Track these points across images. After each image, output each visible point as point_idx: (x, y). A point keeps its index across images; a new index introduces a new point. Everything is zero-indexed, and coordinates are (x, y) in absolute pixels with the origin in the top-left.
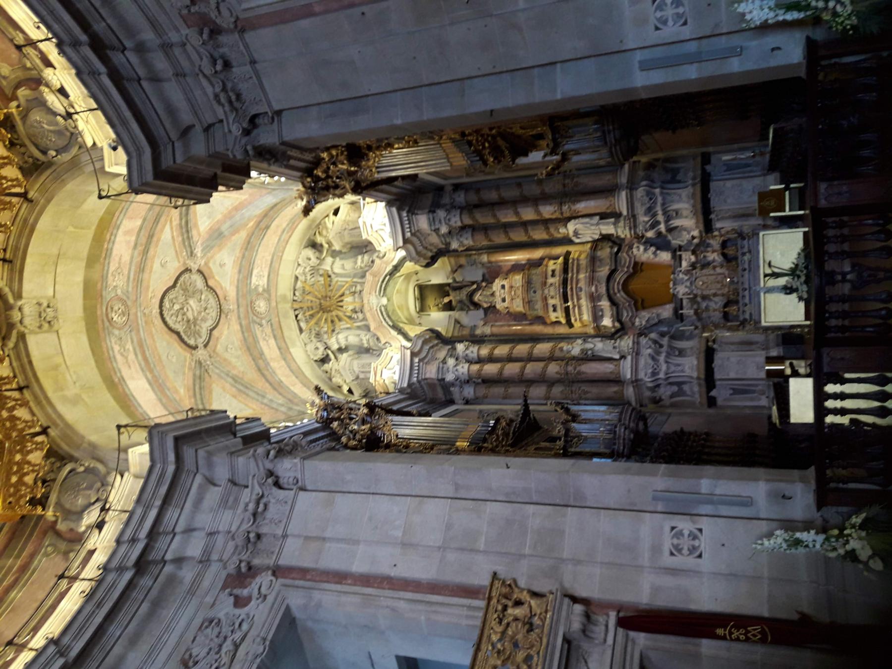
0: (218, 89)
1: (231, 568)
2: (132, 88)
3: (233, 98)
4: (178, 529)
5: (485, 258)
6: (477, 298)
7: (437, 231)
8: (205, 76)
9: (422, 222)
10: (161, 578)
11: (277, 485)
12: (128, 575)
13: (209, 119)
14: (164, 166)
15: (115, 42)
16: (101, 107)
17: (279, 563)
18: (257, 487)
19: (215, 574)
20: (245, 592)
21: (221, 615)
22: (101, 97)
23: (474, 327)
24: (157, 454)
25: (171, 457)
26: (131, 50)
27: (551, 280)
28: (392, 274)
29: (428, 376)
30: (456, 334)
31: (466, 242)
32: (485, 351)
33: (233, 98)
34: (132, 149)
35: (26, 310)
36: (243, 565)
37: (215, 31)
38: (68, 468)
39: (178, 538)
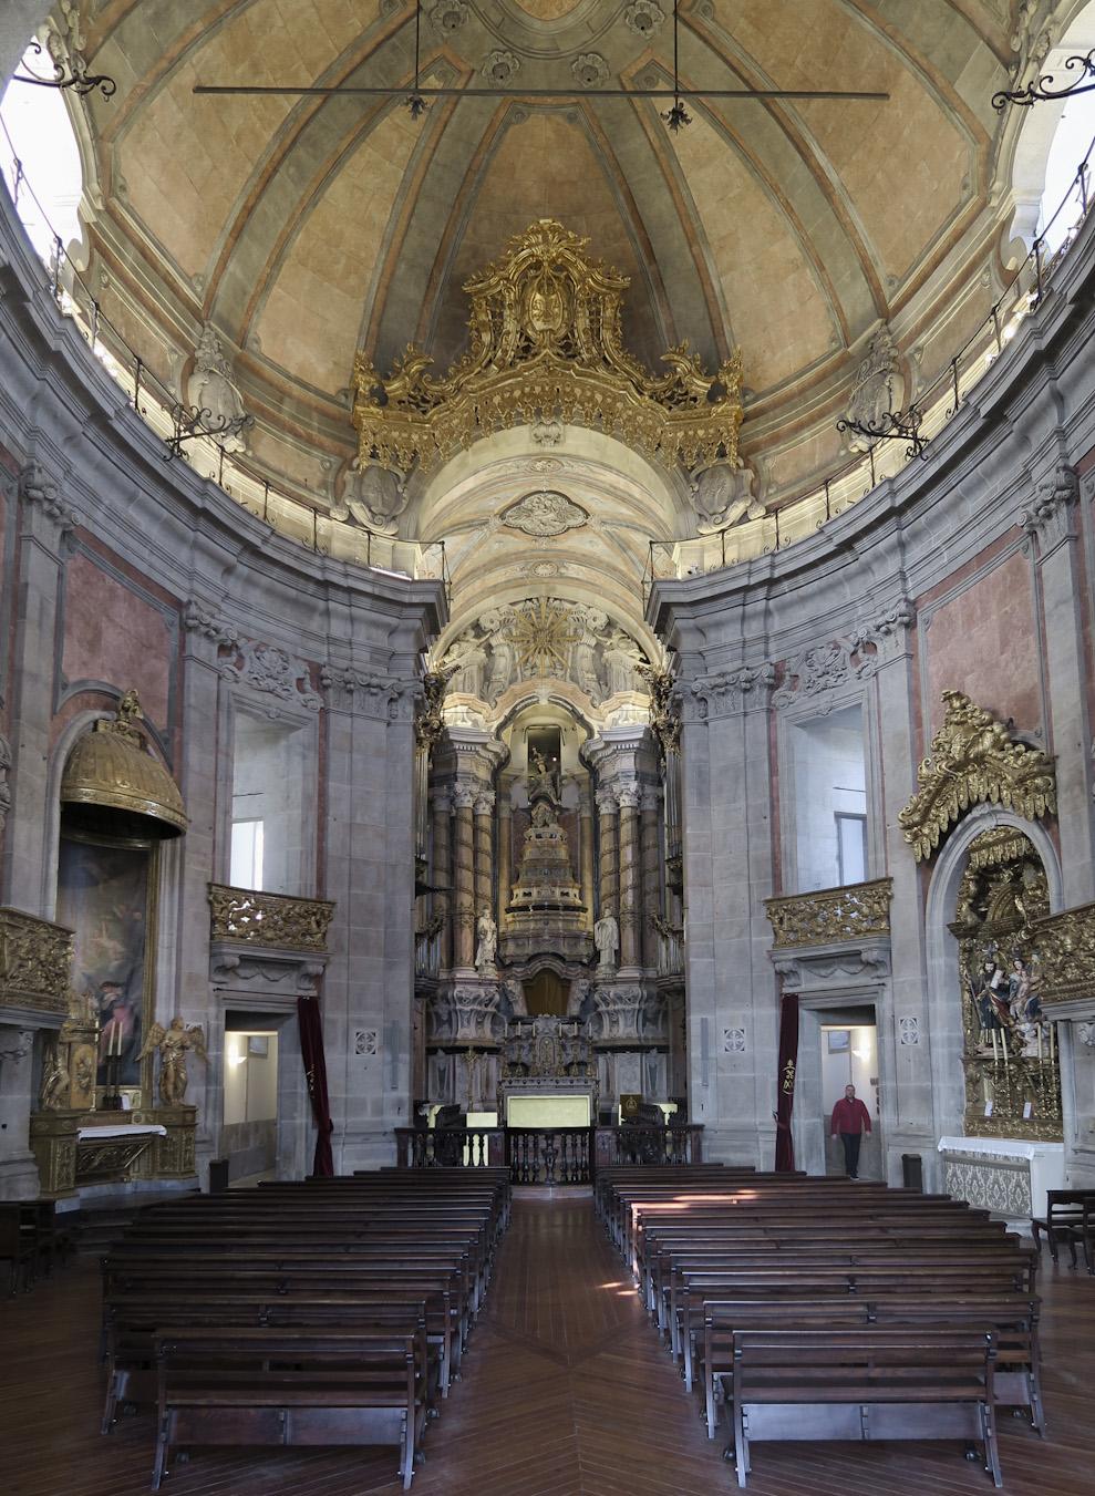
0: (728, 678)
1: (325, 671)
2: (738, 598)
3: (722, 690)
4: (354, 610)
5: (586, 814)
6: (542, 805)
7: (616, 778)
8: (740, 669)
9: (627, 763)
10: (314, 601)
11: (391, 700)
12: (318, 575)
13: (710, 658)
14: (673, 609)
15: (773, 594)
16: (725, 568)
17: (332, 715)
18: (390, 683)
19: (321, 652)
20: (308, 687)
21: (291, 669)
22: (730, 574)
23: (509, 798)
24: (418, 587)
25: (416, 599)
26: (767, 605)
27: (558, 891)
28: (574, 711)
29: (460, 760)
30: (502, 777)
31: (603, 806)
32: (485, 822)
33: (722, 690)
34: (690, 585)
36: (329, 682)
37: (772, 688)
38: (402, 475)
39: (346, 610)
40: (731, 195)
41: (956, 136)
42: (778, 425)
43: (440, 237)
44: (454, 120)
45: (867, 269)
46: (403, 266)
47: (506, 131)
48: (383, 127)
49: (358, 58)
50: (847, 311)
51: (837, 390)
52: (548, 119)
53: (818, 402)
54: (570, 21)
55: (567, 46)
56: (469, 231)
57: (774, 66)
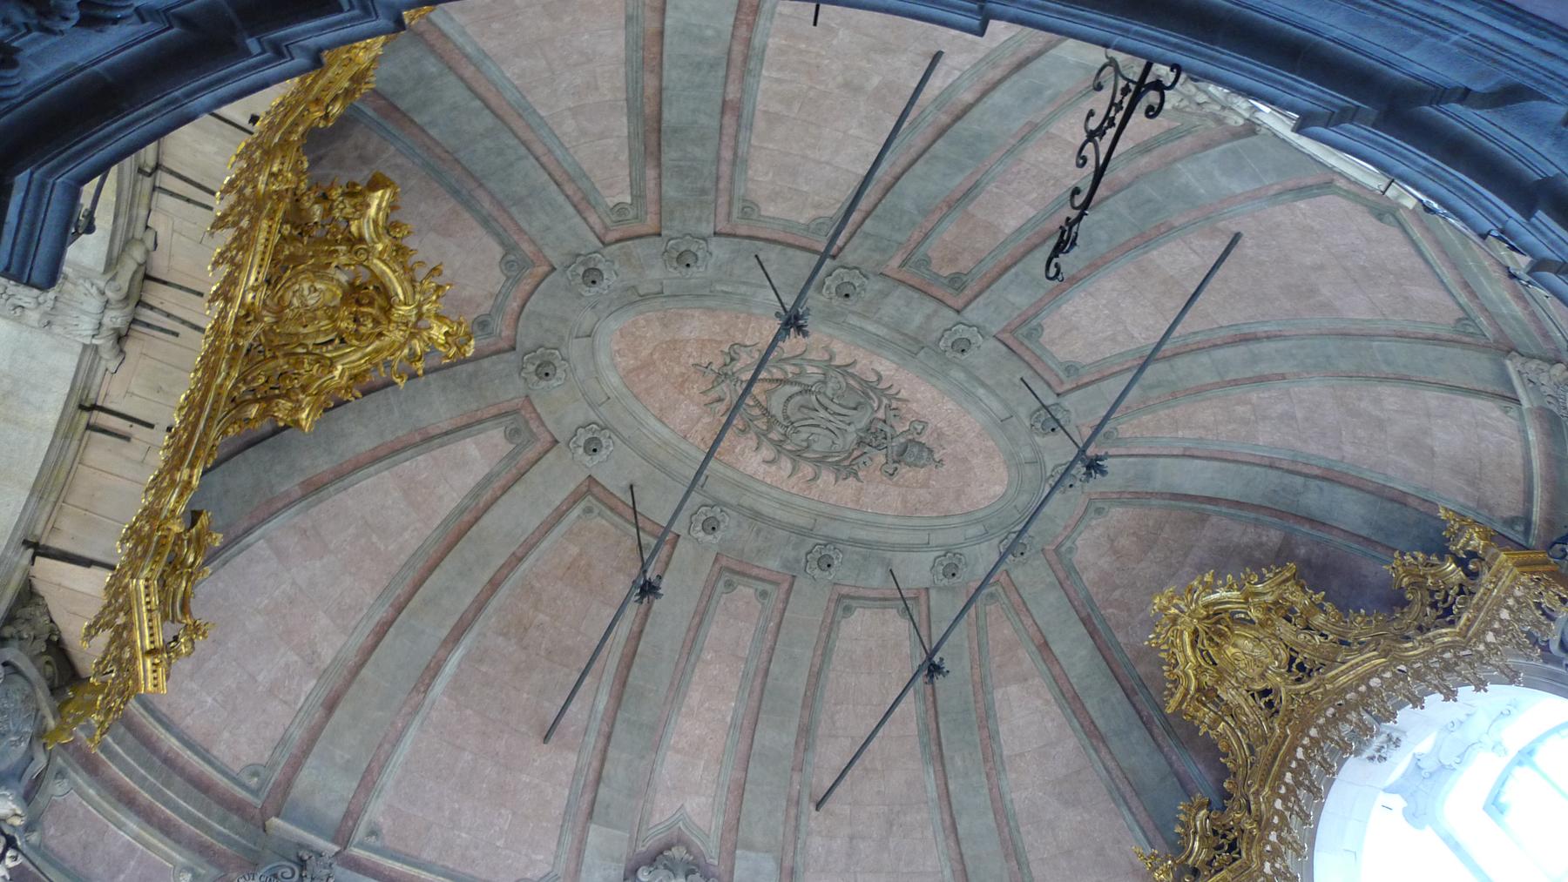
35: (86, 326)
40: (375, 538)
41: (553, 846)
42: (112, 755)
43: (426, 128)
44: (561, 199)
45: (368, 783)
46: (434, 70)
47: (502, 244)
48: (621, 125)
49: (727, 154)
50: (307, 777)
51: (208, 829)
52: (491, 295)
53: (176, 809)
54: (603, 359)
55: (575, 349)
56: (399, 160)
57: (532, 587)
